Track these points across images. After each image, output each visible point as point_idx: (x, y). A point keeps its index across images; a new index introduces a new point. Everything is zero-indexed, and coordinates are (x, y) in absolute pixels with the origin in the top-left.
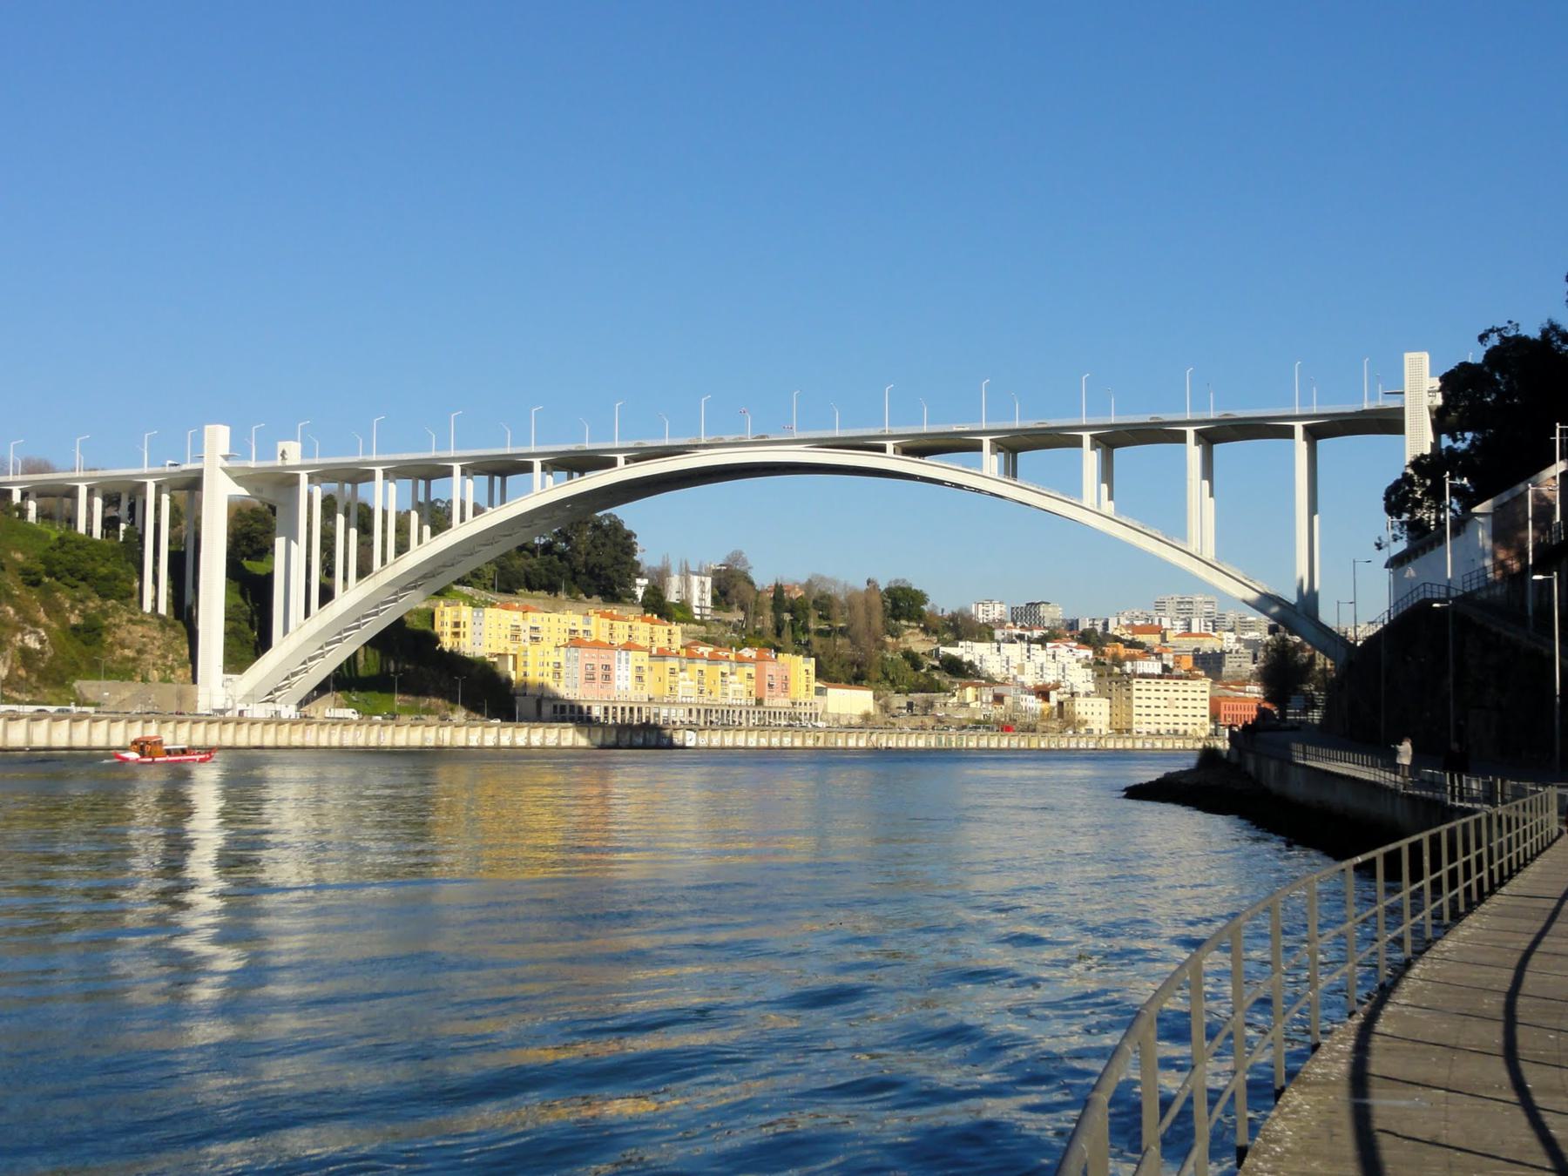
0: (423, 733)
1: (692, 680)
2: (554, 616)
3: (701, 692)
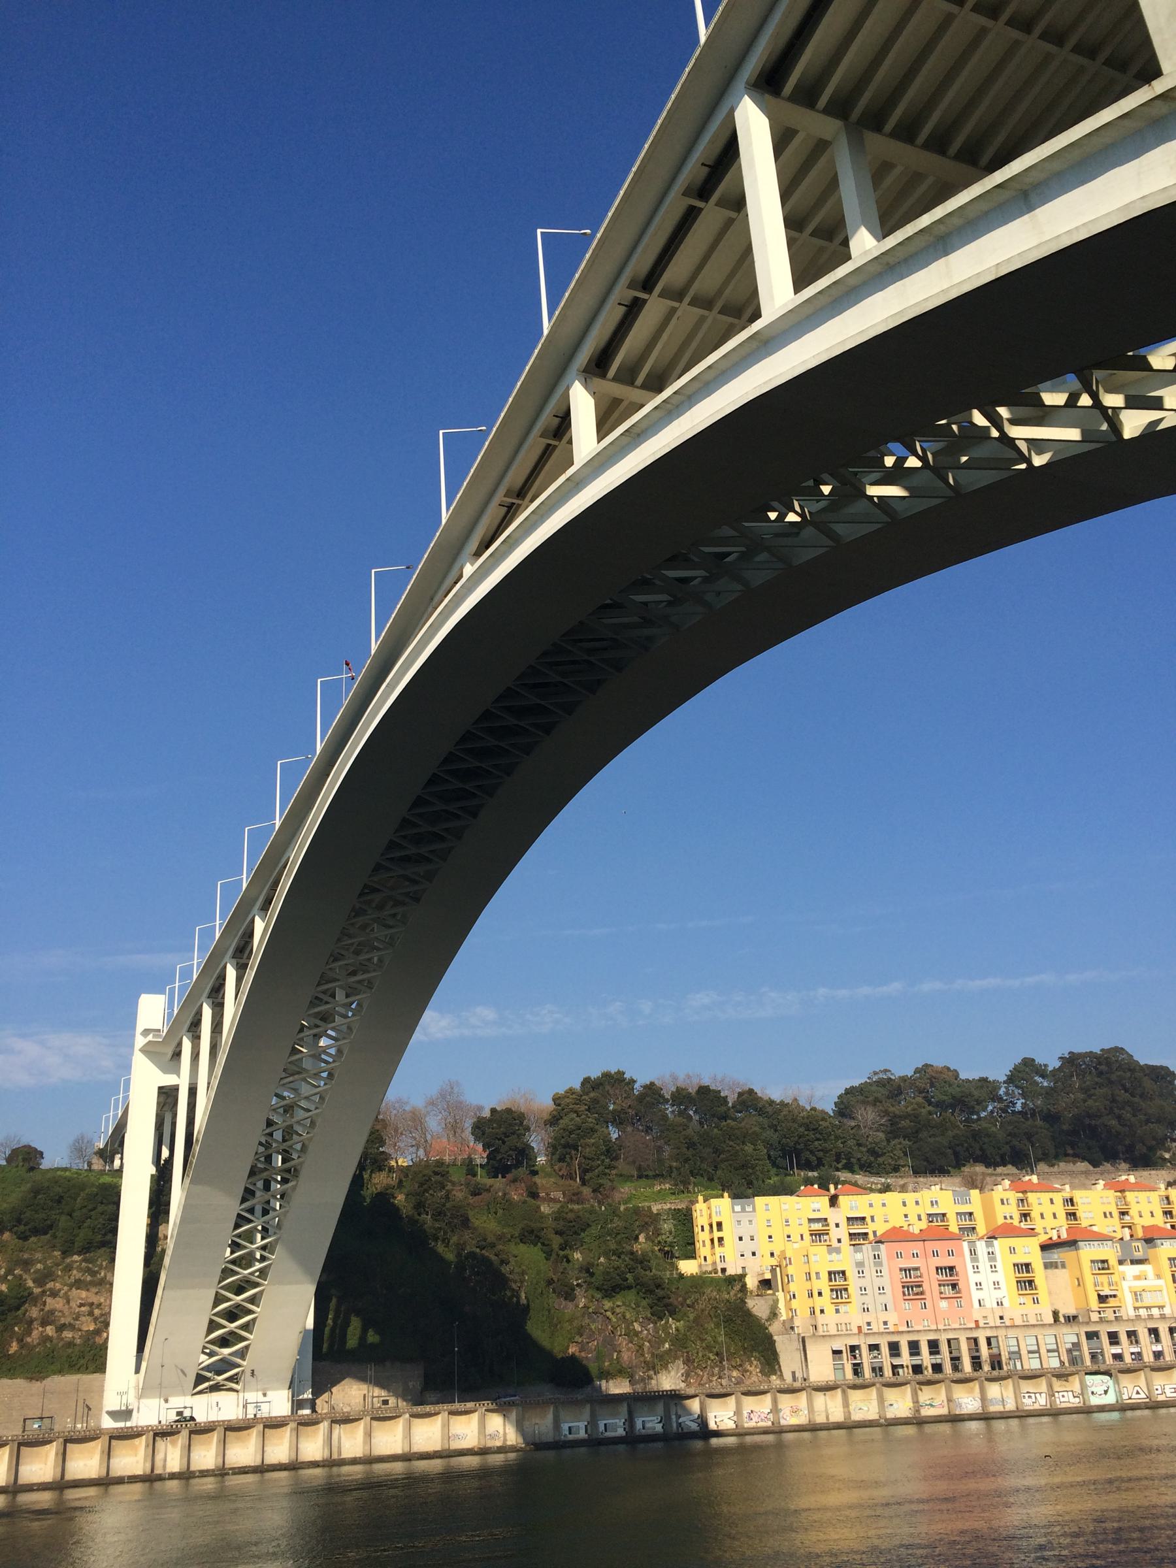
0: (446, 1426)
2: (893, 1198)
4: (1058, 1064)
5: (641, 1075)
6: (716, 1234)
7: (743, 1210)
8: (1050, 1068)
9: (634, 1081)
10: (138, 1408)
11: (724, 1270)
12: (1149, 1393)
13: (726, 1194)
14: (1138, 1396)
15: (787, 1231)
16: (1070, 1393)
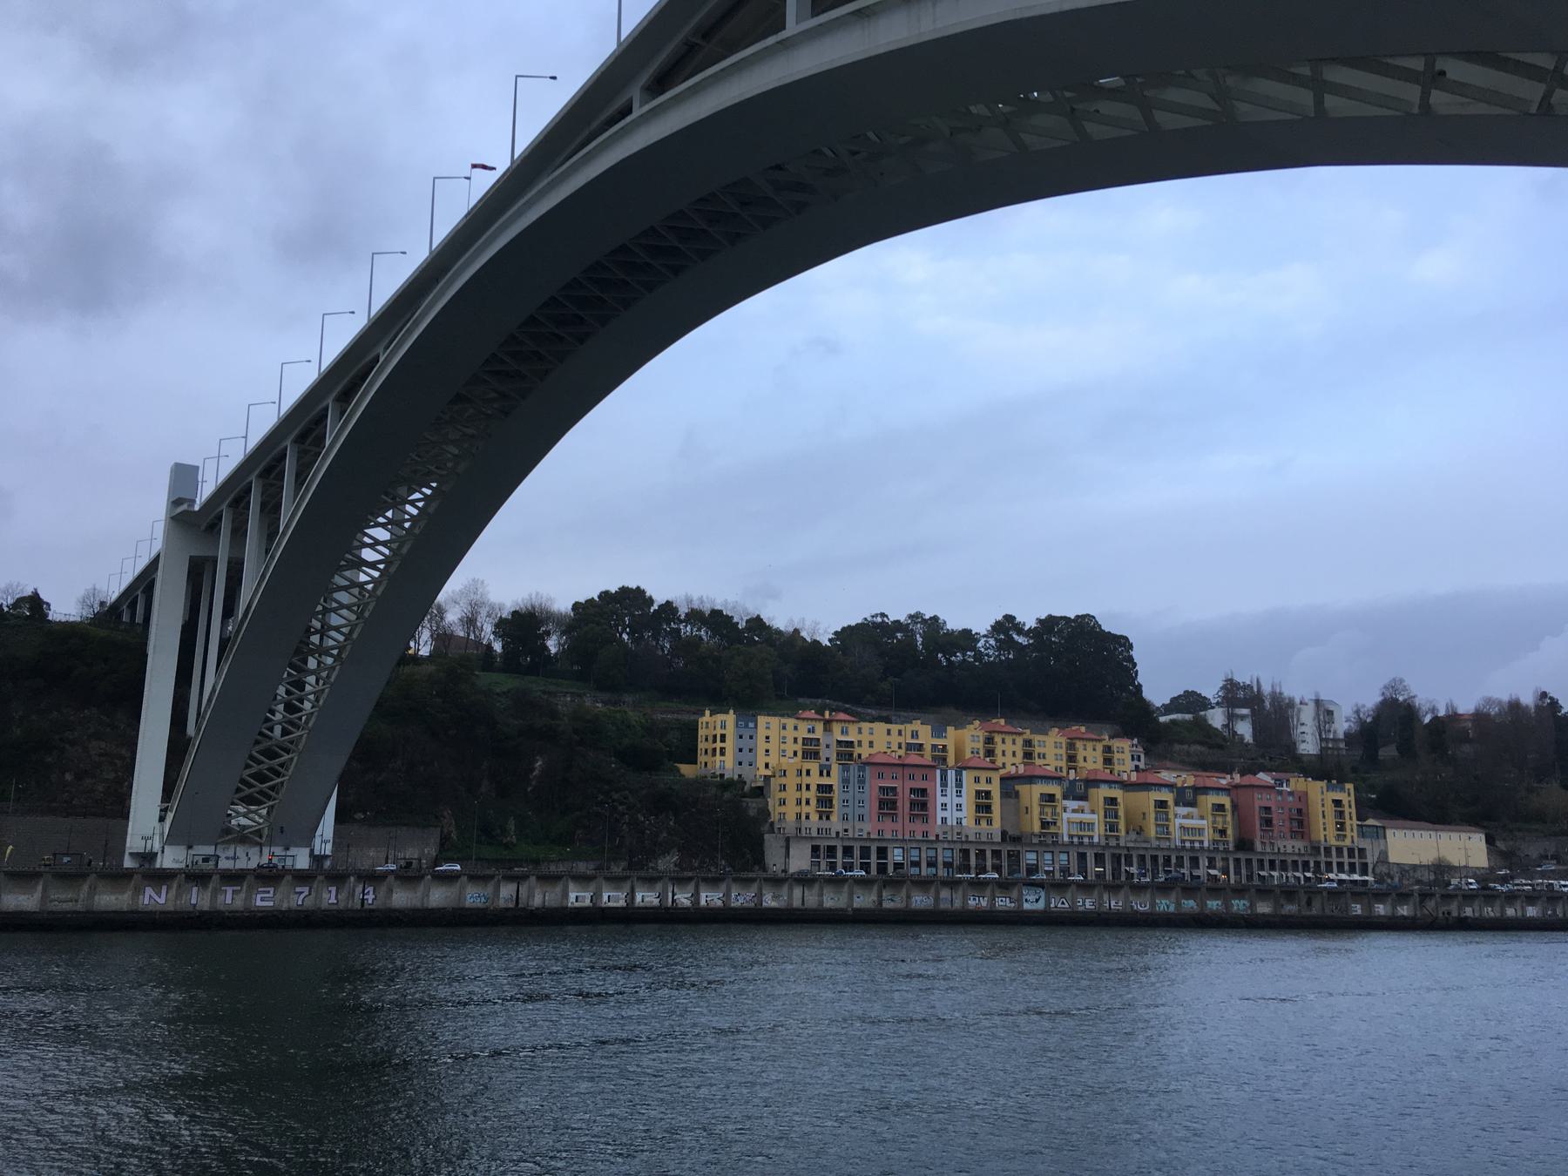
1: (1093, 812)
2: (881, 727)
3: (1113, 827)
4: (1034, 625)
5: (659, 595)
6: (719, 745)
7: (747, 726)
8: (1026, 628)
9: (651, 601)
10: (163, 852)
11: (722, 776)
12: (1073, 903)
13: (731, 712)
14: (1063, 906)
15: (783, 747)
16: (1008, 899)
